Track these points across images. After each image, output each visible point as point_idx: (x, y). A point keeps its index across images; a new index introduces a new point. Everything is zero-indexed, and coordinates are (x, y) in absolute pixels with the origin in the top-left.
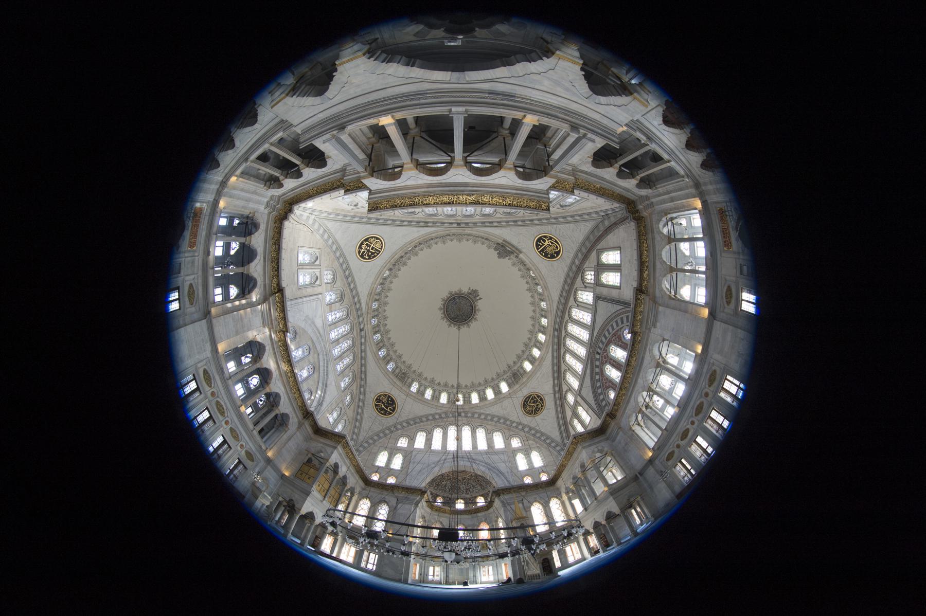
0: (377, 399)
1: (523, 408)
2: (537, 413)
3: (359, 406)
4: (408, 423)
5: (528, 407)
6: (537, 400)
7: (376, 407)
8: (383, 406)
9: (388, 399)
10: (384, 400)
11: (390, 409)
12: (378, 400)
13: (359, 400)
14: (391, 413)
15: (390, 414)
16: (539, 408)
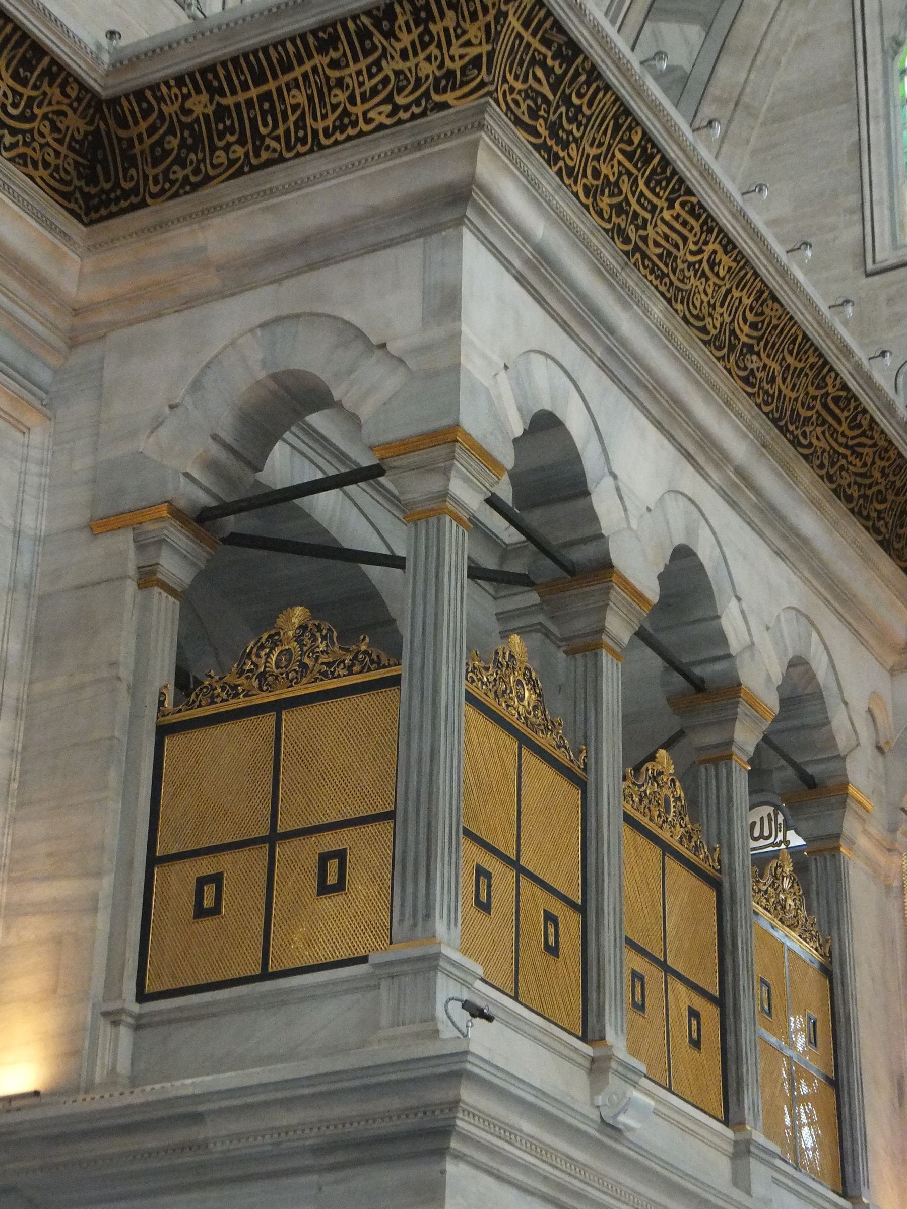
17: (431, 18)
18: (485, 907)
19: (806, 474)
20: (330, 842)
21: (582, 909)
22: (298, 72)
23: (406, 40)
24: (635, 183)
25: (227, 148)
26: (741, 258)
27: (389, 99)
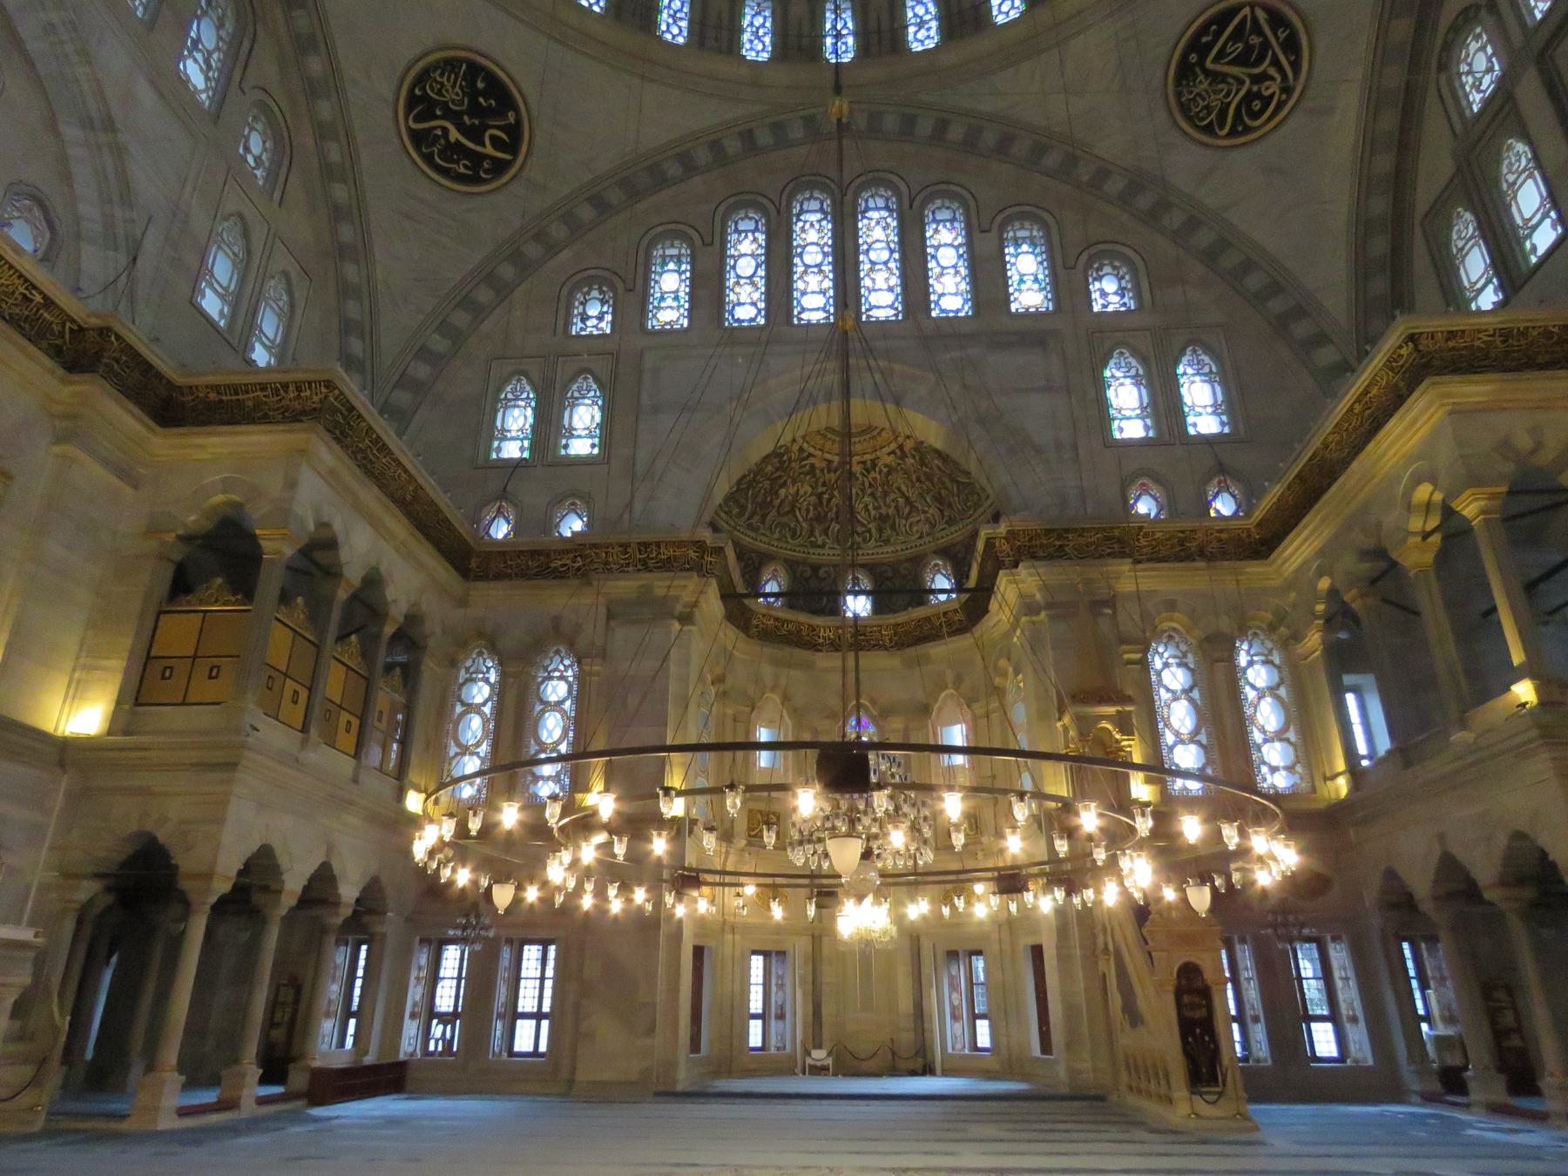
0: (412, 101)
1: (1179, 95)
2: (1248, 130)
3: (329, 173)
4: (599, 203)
5: (1203, 84)
6: (1266, 45)
7: (417, 146)
8: (454, 135)
9: (473, 84)
10: (453, 93)
11: (493, 138)
12: (420, 103)
13: (323, 132)
14: (505, 165)
15: (499, 167)
16: (1267, 101)
17: (301, 391)
18: (270, 689)
19: (428, 545)
20: (216, 661)
21: (310, 689)
22: (251, 395)
23: (292, 395)
24: (372, 450)
25: (220, 414)
26: (410, 475)
27: (283, 413)
